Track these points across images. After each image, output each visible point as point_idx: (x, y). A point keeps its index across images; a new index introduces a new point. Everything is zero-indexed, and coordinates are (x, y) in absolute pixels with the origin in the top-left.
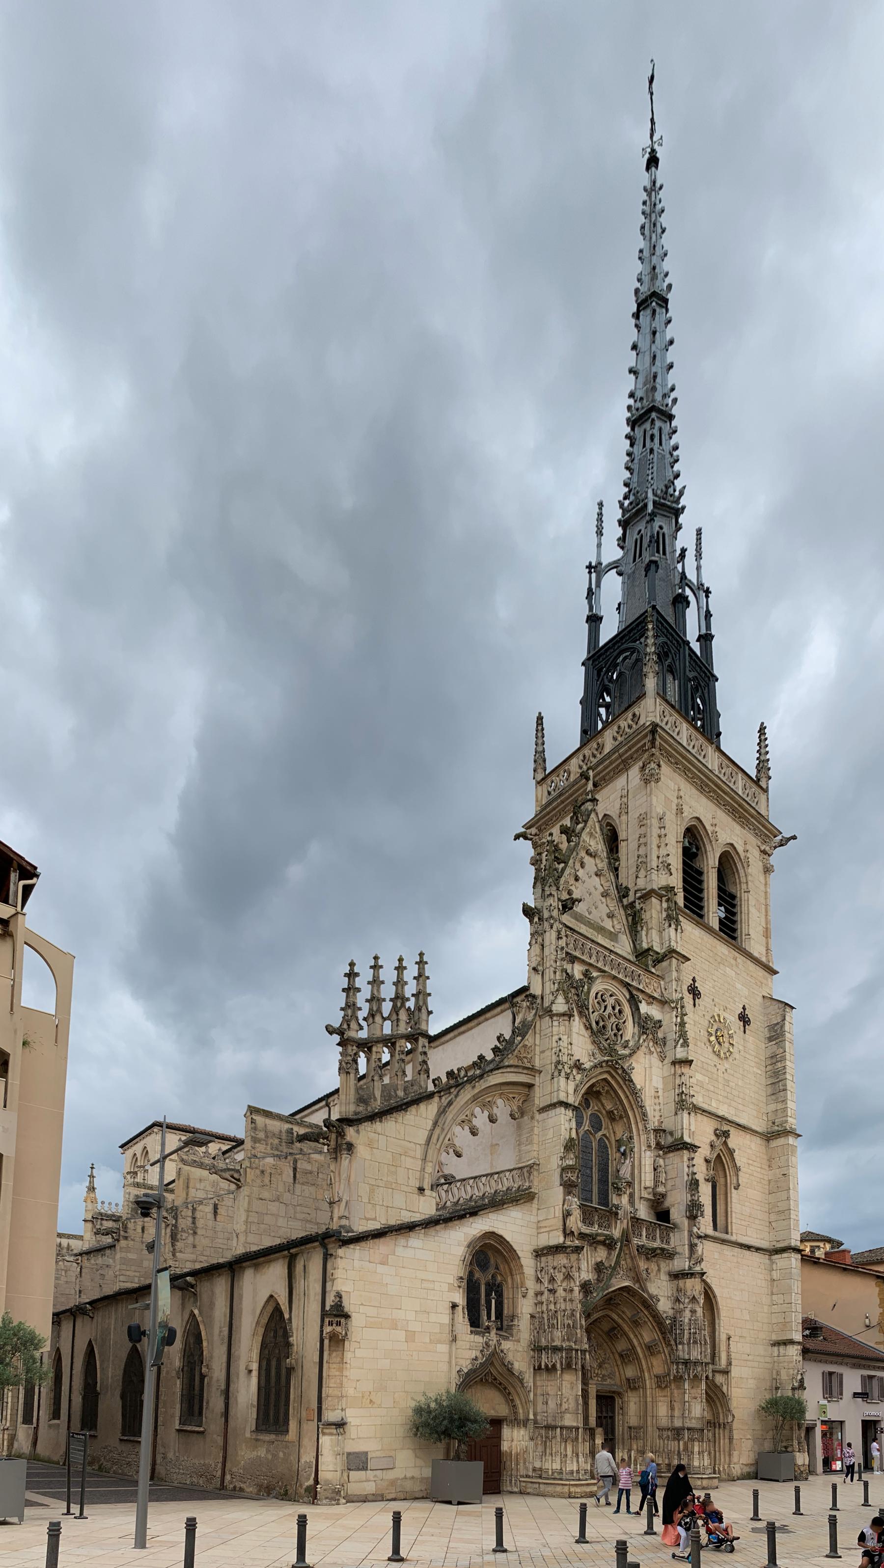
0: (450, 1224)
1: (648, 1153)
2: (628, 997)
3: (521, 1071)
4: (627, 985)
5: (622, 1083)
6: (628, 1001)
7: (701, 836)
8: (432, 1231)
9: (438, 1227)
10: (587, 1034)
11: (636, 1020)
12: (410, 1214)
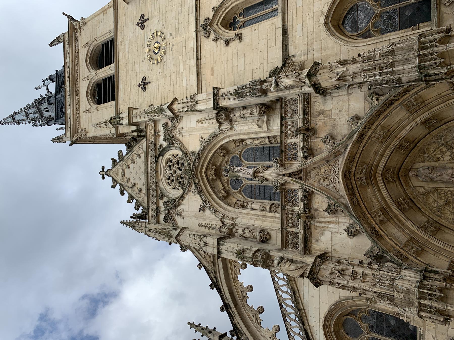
1: (236, 128)
2: (161, 157)
3: (217, 266)
5: (203, 158)
6: (163, 156)
7: (92, 88)
10: (187, 197)
11: (169, 149)
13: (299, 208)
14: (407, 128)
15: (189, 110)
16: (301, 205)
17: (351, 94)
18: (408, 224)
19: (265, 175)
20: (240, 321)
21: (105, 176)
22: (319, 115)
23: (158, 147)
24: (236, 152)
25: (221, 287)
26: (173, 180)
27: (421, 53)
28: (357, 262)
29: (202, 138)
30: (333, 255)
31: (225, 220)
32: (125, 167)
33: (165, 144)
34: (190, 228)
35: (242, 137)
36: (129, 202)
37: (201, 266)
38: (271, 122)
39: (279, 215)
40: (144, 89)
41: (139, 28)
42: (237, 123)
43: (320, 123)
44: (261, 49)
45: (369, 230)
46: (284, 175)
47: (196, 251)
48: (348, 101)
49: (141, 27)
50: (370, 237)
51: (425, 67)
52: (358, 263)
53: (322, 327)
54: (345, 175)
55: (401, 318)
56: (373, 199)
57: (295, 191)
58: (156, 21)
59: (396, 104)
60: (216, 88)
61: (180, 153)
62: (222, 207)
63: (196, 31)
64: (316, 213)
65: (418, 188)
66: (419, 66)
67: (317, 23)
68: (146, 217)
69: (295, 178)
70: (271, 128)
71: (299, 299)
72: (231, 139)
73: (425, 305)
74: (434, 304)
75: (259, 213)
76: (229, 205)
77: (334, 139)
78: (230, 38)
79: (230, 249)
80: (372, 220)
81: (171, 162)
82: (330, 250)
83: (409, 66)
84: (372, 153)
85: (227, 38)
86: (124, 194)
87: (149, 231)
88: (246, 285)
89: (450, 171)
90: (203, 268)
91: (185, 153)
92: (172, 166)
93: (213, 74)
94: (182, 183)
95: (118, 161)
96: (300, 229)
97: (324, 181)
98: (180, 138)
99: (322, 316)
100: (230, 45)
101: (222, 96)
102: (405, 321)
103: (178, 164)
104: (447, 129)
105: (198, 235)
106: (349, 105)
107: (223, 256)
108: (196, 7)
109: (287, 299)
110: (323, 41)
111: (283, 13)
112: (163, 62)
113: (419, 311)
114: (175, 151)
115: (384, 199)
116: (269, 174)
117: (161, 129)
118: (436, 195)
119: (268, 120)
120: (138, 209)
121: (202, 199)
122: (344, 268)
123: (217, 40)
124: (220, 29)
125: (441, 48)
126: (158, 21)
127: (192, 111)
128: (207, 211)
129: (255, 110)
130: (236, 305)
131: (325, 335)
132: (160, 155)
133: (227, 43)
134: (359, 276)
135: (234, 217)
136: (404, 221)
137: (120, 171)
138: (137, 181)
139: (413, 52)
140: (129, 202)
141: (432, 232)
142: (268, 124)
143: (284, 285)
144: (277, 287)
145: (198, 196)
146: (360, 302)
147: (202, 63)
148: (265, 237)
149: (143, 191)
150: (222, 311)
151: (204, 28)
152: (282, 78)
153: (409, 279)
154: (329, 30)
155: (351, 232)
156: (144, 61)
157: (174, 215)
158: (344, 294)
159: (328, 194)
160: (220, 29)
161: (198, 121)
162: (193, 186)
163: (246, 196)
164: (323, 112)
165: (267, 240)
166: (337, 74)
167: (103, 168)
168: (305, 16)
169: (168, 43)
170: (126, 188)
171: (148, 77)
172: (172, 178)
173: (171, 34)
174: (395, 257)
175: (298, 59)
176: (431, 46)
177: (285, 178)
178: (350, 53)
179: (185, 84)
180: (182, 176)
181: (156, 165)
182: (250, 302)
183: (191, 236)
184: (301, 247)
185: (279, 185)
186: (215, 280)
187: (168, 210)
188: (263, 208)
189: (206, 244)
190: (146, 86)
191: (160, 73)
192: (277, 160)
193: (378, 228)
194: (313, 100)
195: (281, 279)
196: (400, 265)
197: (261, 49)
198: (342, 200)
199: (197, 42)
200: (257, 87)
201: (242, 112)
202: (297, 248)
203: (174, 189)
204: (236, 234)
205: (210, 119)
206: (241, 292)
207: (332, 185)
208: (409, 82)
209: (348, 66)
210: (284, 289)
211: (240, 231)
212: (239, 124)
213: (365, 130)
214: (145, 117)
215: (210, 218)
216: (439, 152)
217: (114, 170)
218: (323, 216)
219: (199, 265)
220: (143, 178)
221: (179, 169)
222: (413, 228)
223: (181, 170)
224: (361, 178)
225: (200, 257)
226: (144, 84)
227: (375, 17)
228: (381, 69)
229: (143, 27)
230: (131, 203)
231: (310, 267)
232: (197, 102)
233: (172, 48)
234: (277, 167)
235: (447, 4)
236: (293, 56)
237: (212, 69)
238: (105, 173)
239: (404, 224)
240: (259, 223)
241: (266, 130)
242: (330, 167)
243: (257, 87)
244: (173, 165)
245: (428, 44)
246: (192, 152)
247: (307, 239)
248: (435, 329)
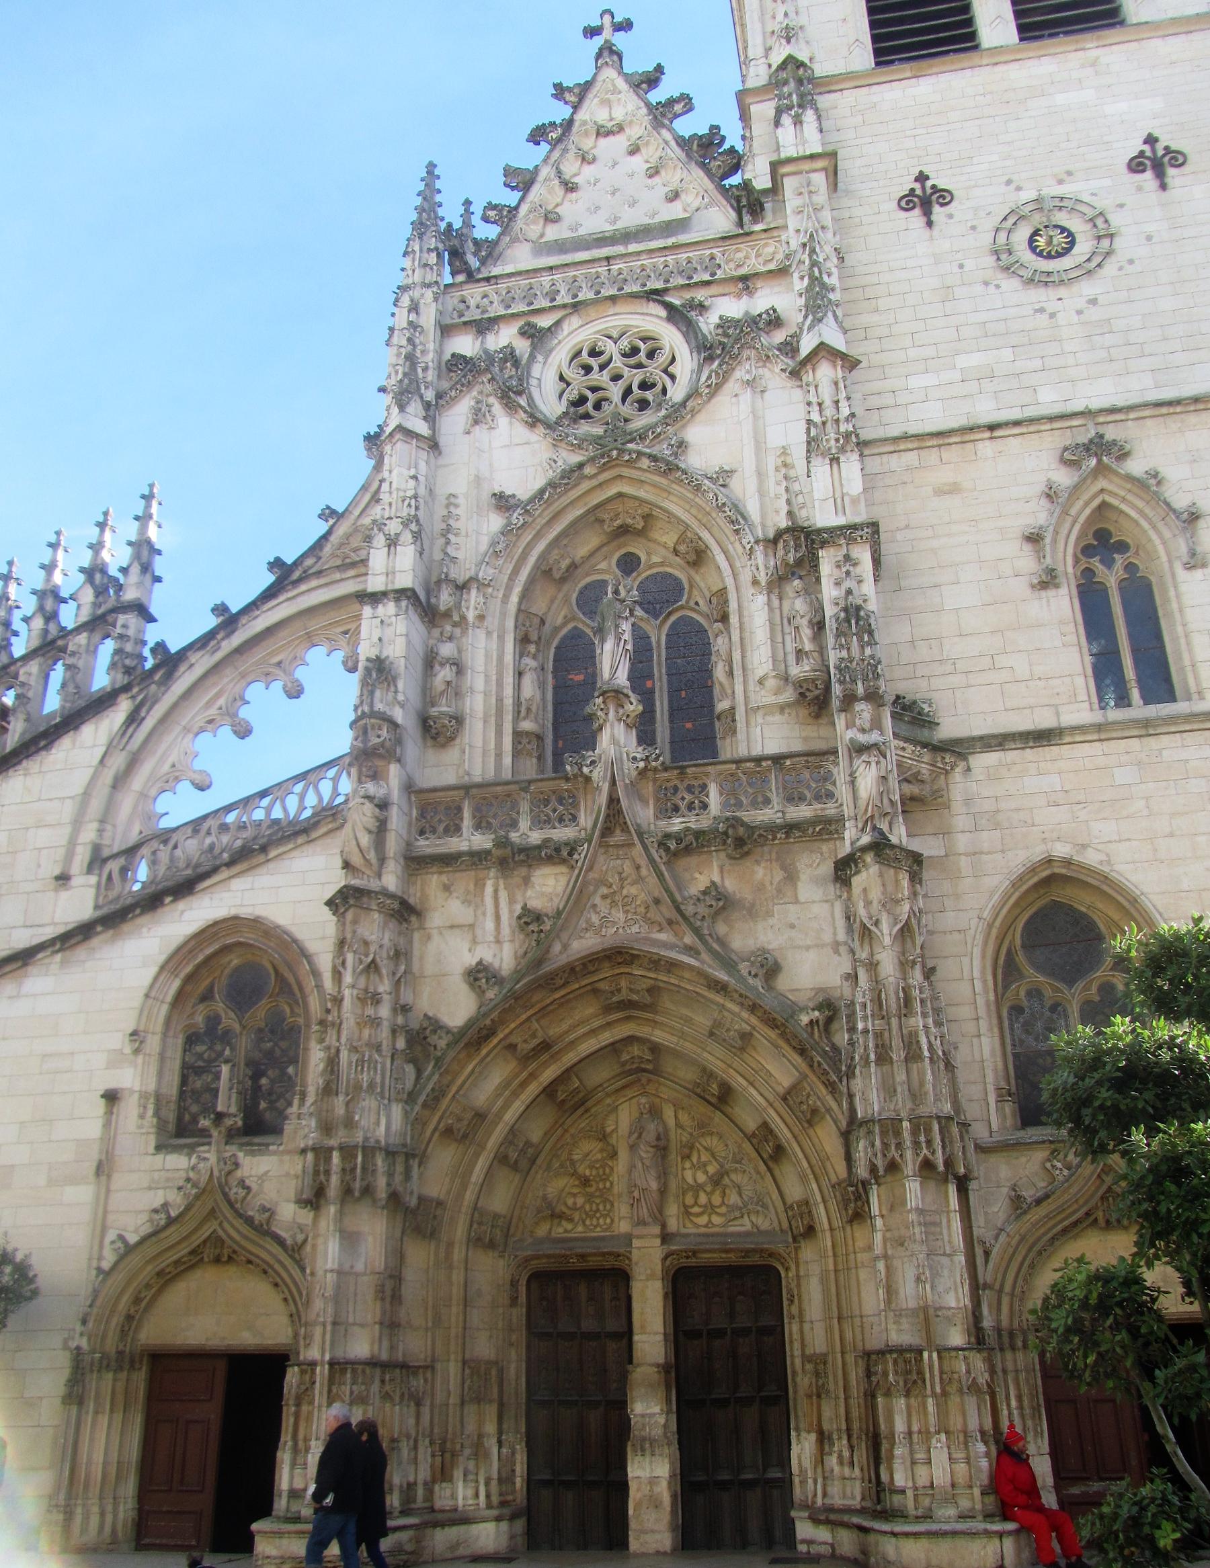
0: (126, 927)
2: (663, 313)
4: (654, 295)
8: (81, 952)
9: (95, 942)
12: (30, 932)
13: (528, 833)
14: (752, 1090)
15: (813, 432)
16: (536, 837)
17: (837, 952)
18: (518, 1106)
19: (612, 726)
20: (198, 671)
21: (598, 41)
22: (783, 868)
23: (700, 295)
24: (695, 592)
25: (281, 598)
26: (588, 369)
27: (906, 1124)
28: (407, 997)
29: (729, 473)
30: (416, 936)
31: (474, 592)
32: (634, 132)
33: (708, 323)
34: (441, 461)
35: (734, 620)
36: (509, 172)
37: (331, 522)
38: (777, 718)
39: (507, 774)
40: (908, 202)
41: (1135, 146)
42: (776, 602)
43: (760, 872)
44: (1002, 661)
45: (488, 1022)
46: (613, 783)
47: (371, 492)
48: (817, 946)
49: (1142, 154)
50: (470, 1023)
51: (870, 1132)
52: (402, 1002)
53: (233, 912)
54: (620, 953)
55: (296, 1102)
56: (570, 1022)
57: (574, 818)
58: (1150, 228)
59: (803, 1066)
60: (877, 532)
61: (677, 393)
62: (516, 572)
63: (1087, 413)
64: (518, 880)
65: (612, 1117)
66: (873, 1121)
67: (1055, 835)
68: (459, 272)
69: (608, 816)
70: (760, 720)
71: (291, 846)
72: (729, 582)
73: (328, 1159)
74: (335, 1180)
75: (509, 702)
76: (524, 596)
77: (717, 913)
78: (1048, 548)
79: (389, 633)
80: (513, 1026)
81: (651, 355)
82: (428, 924)
83: (875, 1097)
84: (685, 1011)
85: (1048, 540)
86: (537, 143)
87: (414, 308)
88: (300, 673)
89: (654, 1185)
90: (323, 527)
91: (679, 413)
92: (632, 361)
93: (940, 492)
94: (581, 410)
95: (657, 96)
96: (471, 839)
97: (604, 897)
98: (731, 386)
99: (259, 911)
100: (1028, 548)
101: (847, 558)
102: (290, 1110)
103: (644, 386)
104: (758, 1173)
105: (417, 508)
106: (808, 948)
107: (367, 611)
108: (1170, 403)
109: (285, 809)
110: (999, 856)
111: (1099, 727)
112: (1000, 275)
113: (314, 1149)
114: (686, 364)
115: (573, 1044)
116: (614, 741)
117: (763, 300)
118: (599, 1156)
119: (782, 708)
120: (486, 219)
121: (531, 500)
122: (384, 971)
123: (1048, 496)
124: (1087, 504)
125: (910, 1163)
126: (1149, 238)
127: (809, 443)
128: (495, 522)
129: (807, 668)
130: (239, 650)
131: (216, 923)
132: (669, 307)
133: (1034, 538)
134: (370, 1011)
135: (489, 619)
136: (523, 1097)
137: (619, 114)
138: (583, 197)
139: (909, 1105)
140: (509, 172)
141: (506, 1157)
142: (769, 709)
143: (321, 799)
144: (312, 777)
145: (539, 483)
146: (314, 1005)
147: (980, 445)
148: (438, 730)
149: (553, 233)
150: (213, 610)
151: (1095, 448)
152: (878, 763)
153: (382, 1122)
154: (1033, 870)
155: (478, 975)
156: (1012, 187)
157: (475, 393)
158: (325, 963)
159: (569, 913)
160: (1087, 504)
161: (784, 452)
162: (575, 458)
163: (563, 640)
164: (791, 877)
165: (434, 738)
166: (877, 923)
167: (625, 26)
168: (1082, 798)
169: (1062, 292)
170: (556, 154)
171: (950, 216)
172: (596, 368)
173: (1093, 302)
174: (430, 1086)
175: (959, 786)
176: (916, 1144)
177: (606, 787)
178: (956, 936)
179: (915, 382)
180: (605, 404)
181: (634, 296)
182: (255, 691)
183: (412, 483)
184: (426, 846)
185: (586, 770)
186: (296, 575)
187: (487, 370)
188: (523, 714)
189: (392, 542)
190: (917, 211)
191: (961, 266)
192: (656, 760)
193: (495, 1041)
194: (825, 848)
195: (335, 788)
196: (411, 1098)
197: (1002, 661)
198: (557, 947)
199: (1052, 419)
200: (860, 684)
201: (805, 622)
202: (422, 833)
203: (562, 378)
204: (436, 632)
205: (788, 502)
206: (279, 664)
207: (595, 919)
208: (851, 1096)
209: (897, 948)
210: (311, 800)
211: (446, 650)
212: (771, 609)
213: (736, 996)
214: (798, 231)
215: (478, 531)
216: (703, 1159)
217: (621, 84)
218: (512, 901)
219: (333, 512)
220: (596, 224)
221: (628, 392)
222: (510, 1116)
223: (624, 400)
224: (619, 990)
225: (357, 513)
226: (925, 199)
227: (1059, 990)
228: (878, 1035)
229: (1136, 165)
230: (506, 185)
231: (374, 885)
232: (835, 460)
233: (1041, 310)
234: (635, 758)
235: (1048, 1165)
236: (969, 769)
237: (953, 489)
238: (607, 36)
239: (515, 1094)
240: (476, 704)
241: (753, 705)
242: (642, 910)
243: (860, 684)
244: (640, 366)
245: (922, 1139)
246: (682, 445)
247: (447, 861)
248: (287, 1175)
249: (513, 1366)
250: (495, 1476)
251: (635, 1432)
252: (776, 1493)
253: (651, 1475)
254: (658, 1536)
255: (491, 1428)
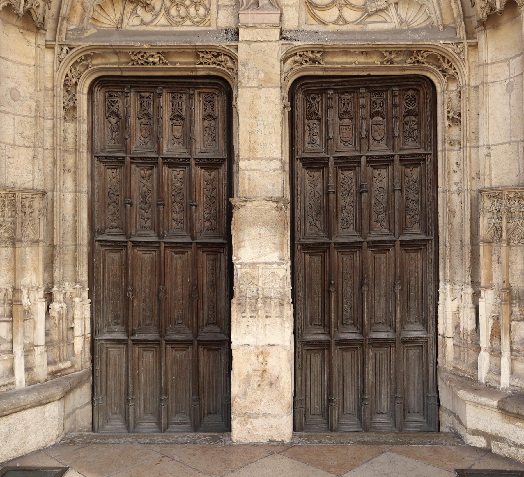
249: (69, 198)
250: (41, 339)
251: (241, 286)
252: (413, 353)
253: (263, 342)
254: (273, 421)
255: (32, 278)
